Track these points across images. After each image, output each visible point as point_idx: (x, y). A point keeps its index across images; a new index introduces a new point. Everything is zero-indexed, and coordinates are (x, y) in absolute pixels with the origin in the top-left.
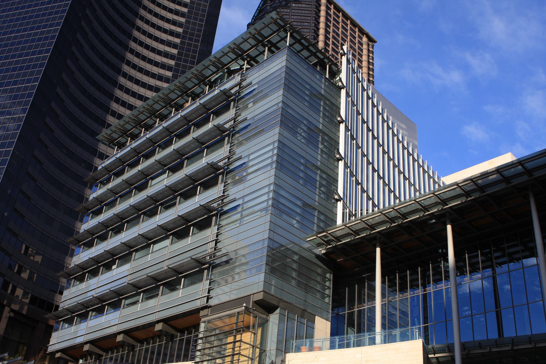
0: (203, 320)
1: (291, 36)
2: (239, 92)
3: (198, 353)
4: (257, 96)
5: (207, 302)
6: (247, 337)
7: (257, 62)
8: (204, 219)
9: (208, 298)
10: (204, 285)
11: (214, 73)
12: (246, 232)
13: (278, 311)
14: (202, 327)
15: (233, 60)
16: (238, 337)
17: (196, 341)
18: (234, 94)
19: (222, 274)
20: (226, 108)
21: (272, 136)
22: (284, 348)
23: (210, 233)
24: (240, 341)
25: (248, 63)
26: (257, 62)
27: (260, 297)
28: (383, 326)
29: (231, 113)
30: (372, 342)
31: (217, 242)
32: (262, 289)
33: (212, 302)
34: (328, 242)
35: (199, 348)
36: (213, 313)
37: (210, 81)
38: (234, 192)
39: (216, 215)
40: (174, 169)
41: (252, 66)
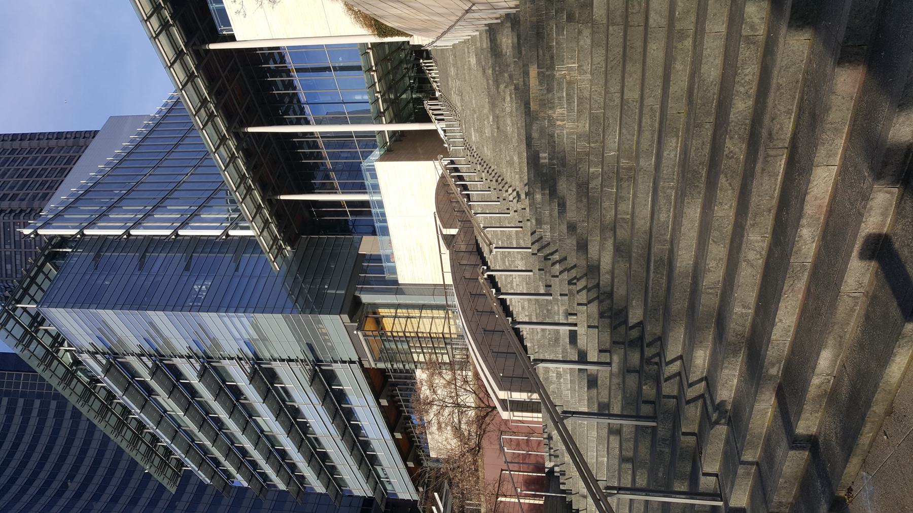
0: (373, 366)
1: (19, 302)
2: (104, 354)
3: (407, 367)
6: (388, 323)
7: (59, 335)
8: (264, 376)
9: (351, 362)
10: (338, 368)
11: (79, 380)
12: (278, 334)
13: (357, 294)
14: (381, 365)
15: (60, 362)
16: (389, 334)
17: (395, 370)
19: (322, 349)
20: (127, 367)
22: (394, 287)
23: (281, 370)
24: (392, 332)
25: (61, 344)
26: (59, 335)
27: (346, 317)
29: (133, 361)
30: (380, 204)
33: (355, 358)
34: (280, 249)
35: (401, 366)
37: (89, 383)
38: (231, 347)
39: (259, 365)
41: (64, 340)
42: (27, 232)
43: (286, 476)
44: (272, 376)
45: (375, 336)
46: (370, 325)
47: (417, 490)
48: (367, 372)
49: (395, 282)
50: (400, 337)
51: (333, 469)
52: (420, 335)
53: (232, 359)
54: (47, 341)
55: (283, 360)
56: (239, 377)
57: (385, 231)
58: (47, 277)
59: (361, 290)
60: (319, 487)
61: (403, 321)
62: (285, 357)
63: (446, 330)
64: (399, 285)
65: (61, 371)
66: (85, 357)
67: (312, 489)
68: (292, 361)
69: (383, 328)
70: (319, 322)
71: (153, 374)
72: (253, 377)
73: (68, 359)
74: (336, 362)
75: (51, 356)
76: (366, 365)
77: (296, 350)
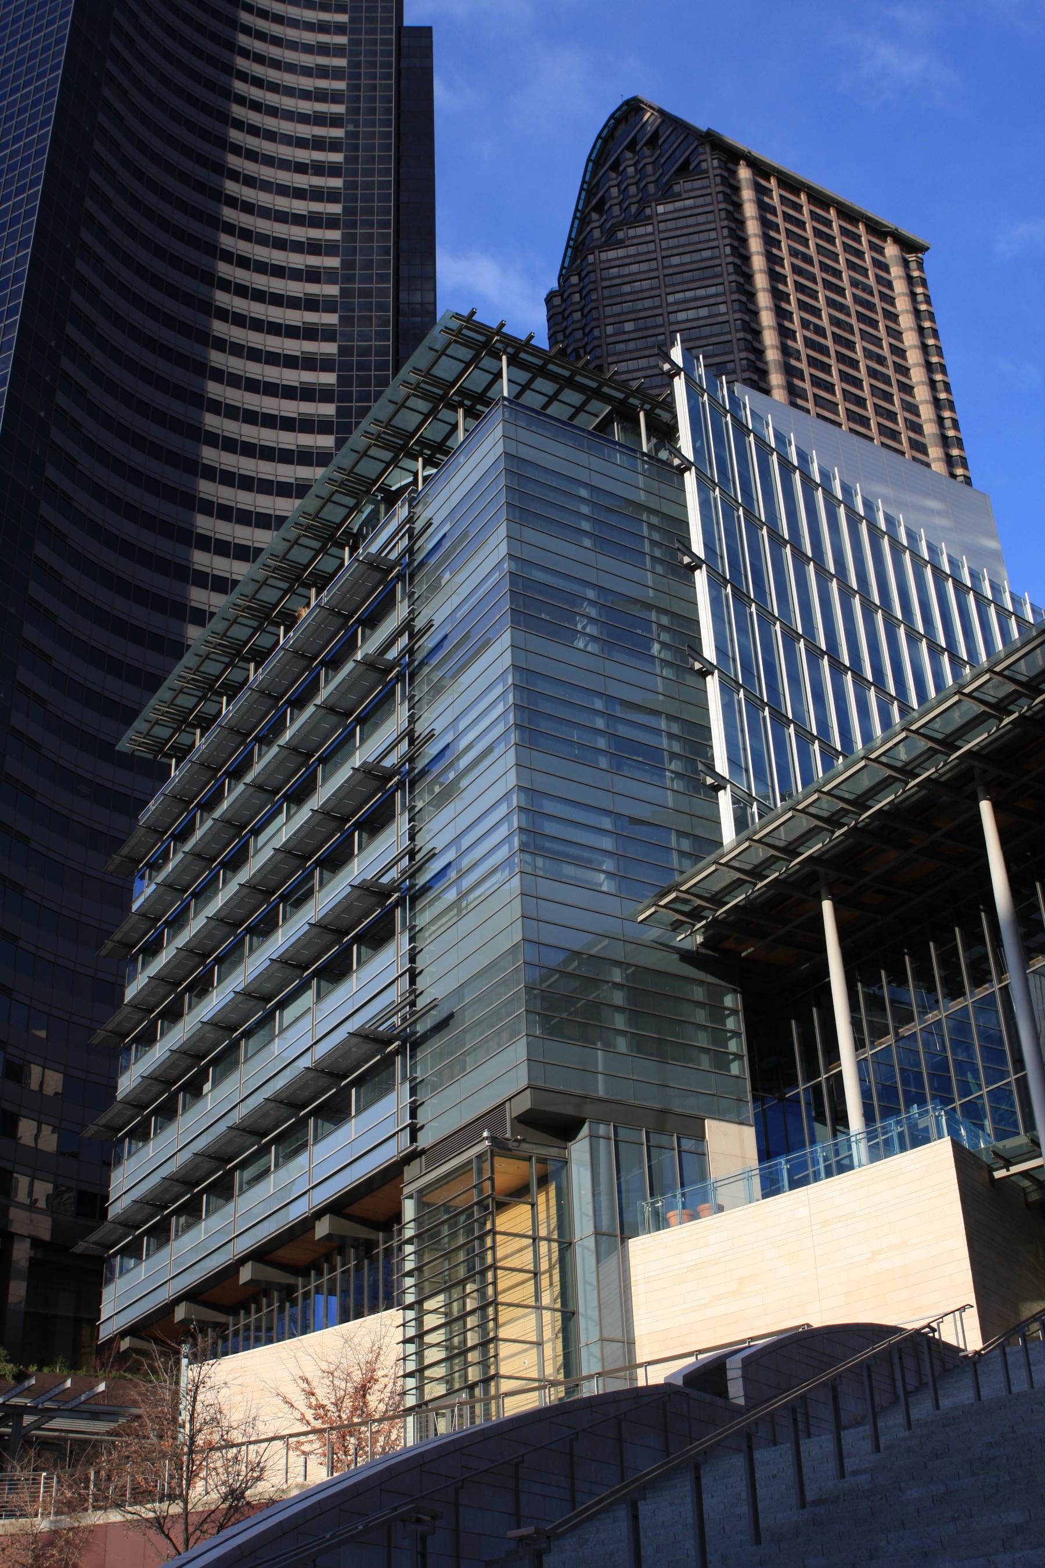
0: (407, 1191)
2: (410, 551)
4: (457, 547)
5: (413, 1139)
6: (515, 1219)
7: (446, 453)
8: (377, 918)
9: (414, 1131)
12: (471, 939)
13: (585, 1130)
14: (409, 1210)
15: (388, 465)
18: (398, 562)
21: (498, 656)
23: (389, 960)
25: (428, 462)
27: (524, 1103)
28: (868, 1116)
30: (844, 1166)
31: (413, 975)
32: (524, 1083)
33: (425, 1140)
34: (696, 915)
35: (409, 1265)
36: (431, 1165)
37: (347, 533)
38: (439, 831)
40: (299, 796)
41: (435, 465)
42: (677, 354)
43: (153, 1000)
44: (378, 937)
45: (478, 1187)
46: (507, 1172)
47: (123, 1334)
48: (391, 1175)
49: (626, 1231)
50: (482, 1256)
51: (168, 1113)
52: (491, 1310)
53: (412, 838)
54: (432, 431)
55: (412, 959)
56: (374, 859)
57: (771, 1187)
58: (579, 409)
59: (593, 1137)
60: (127, 1083)
61: (526, 1259)
62: (420, 964)
63: (506, 1386)
64: (624, 1239)
65: (368, 469)
66: (402, 512)
67: (126, 1068)
68: (413, 982)
69: (501, 1206)
70: (514, 1033)
71: (370, 664)
72: (372, 892)
73: (398, 480)
74: (413, 1091)
75: (401, 446)
76: (409, 1172)
77: (434, 988)
